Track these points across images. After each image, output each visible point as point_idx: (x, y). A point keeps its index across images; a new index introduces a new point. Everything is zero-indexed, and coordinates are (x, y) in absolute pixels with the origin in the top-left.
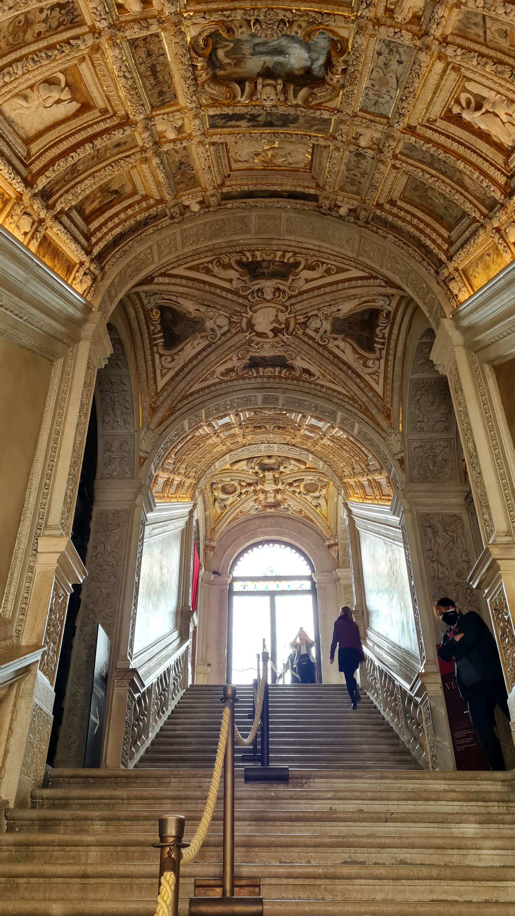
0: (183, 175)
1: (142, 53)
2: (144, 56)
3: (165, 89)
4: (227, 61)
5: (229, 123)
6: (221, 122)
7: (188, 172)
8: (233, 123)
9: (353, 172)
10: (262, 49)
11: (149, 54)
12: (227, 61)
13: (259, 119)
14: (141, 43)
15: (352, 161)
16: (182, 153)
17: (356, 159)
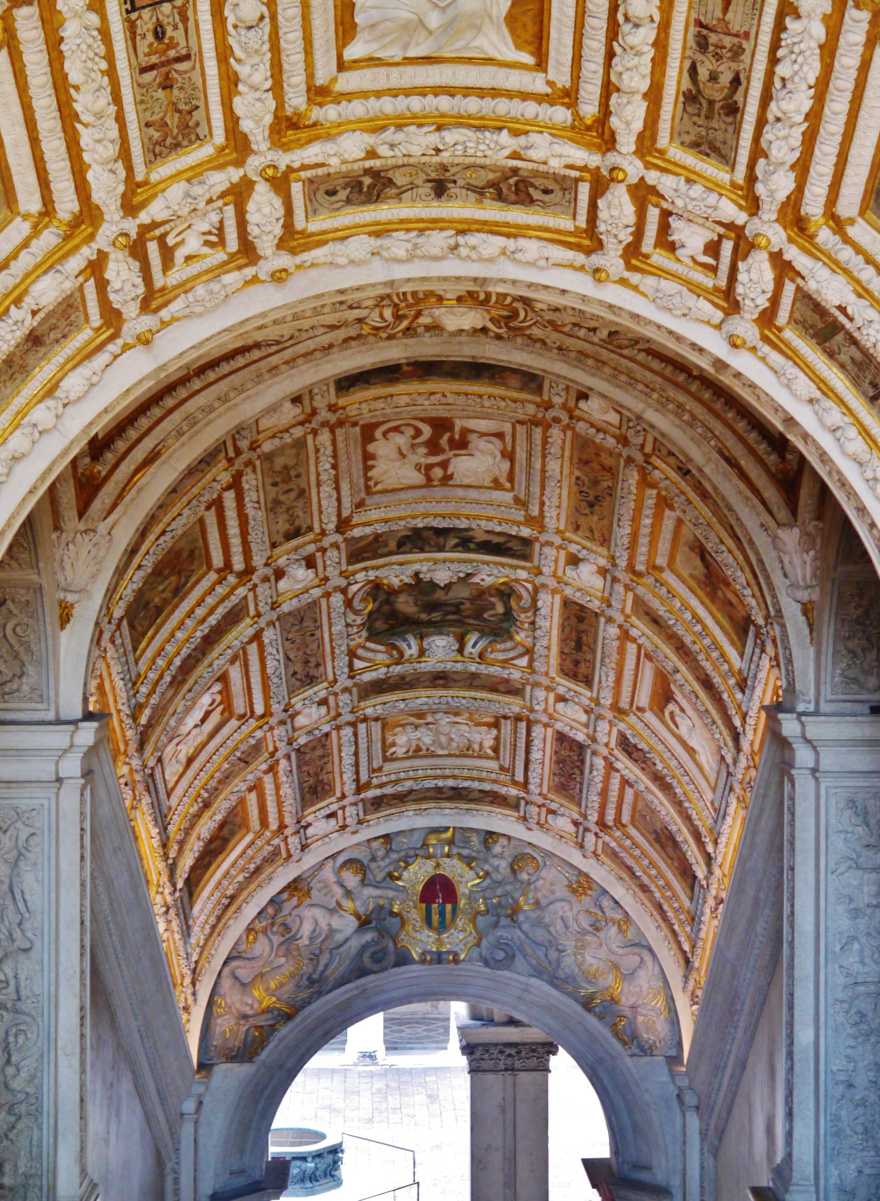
0: (595, 483)
1: (583, 669)
2: (583, 665)
3: (574, 620)
4: (493, 599)
5: (501, 540)
6: (514, 545)
7: (586, 479)
8: (496, 540)
9: (292, 495)
10: (449, 609)
11: (577, 663)
12: (493, 599)
13: (456, 541)
14: (580, 677)
15: (301, 514)
16: (582, 521)
17: (297, 523)
